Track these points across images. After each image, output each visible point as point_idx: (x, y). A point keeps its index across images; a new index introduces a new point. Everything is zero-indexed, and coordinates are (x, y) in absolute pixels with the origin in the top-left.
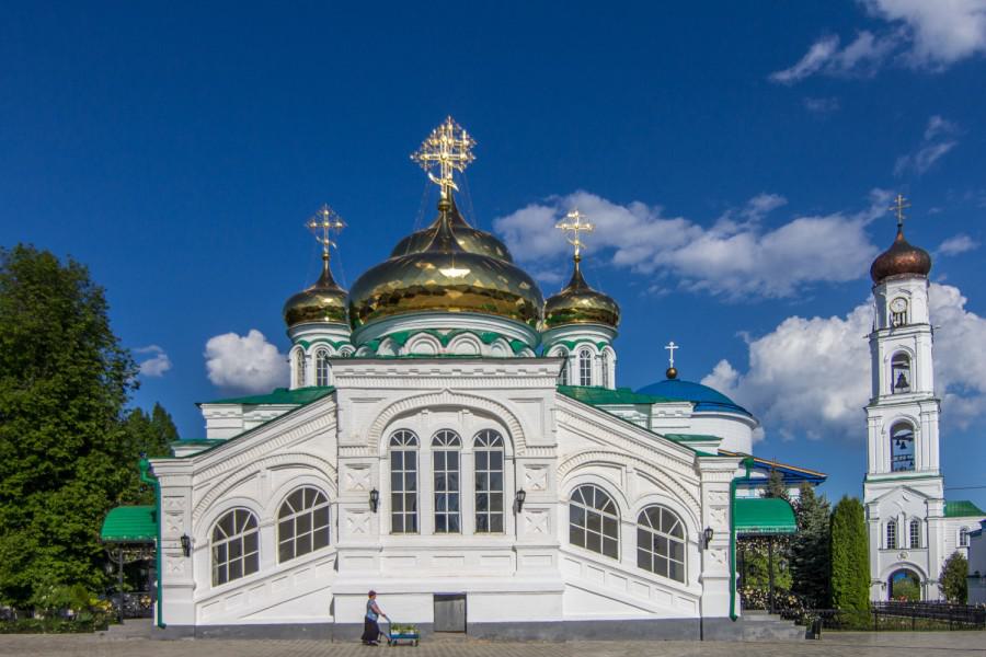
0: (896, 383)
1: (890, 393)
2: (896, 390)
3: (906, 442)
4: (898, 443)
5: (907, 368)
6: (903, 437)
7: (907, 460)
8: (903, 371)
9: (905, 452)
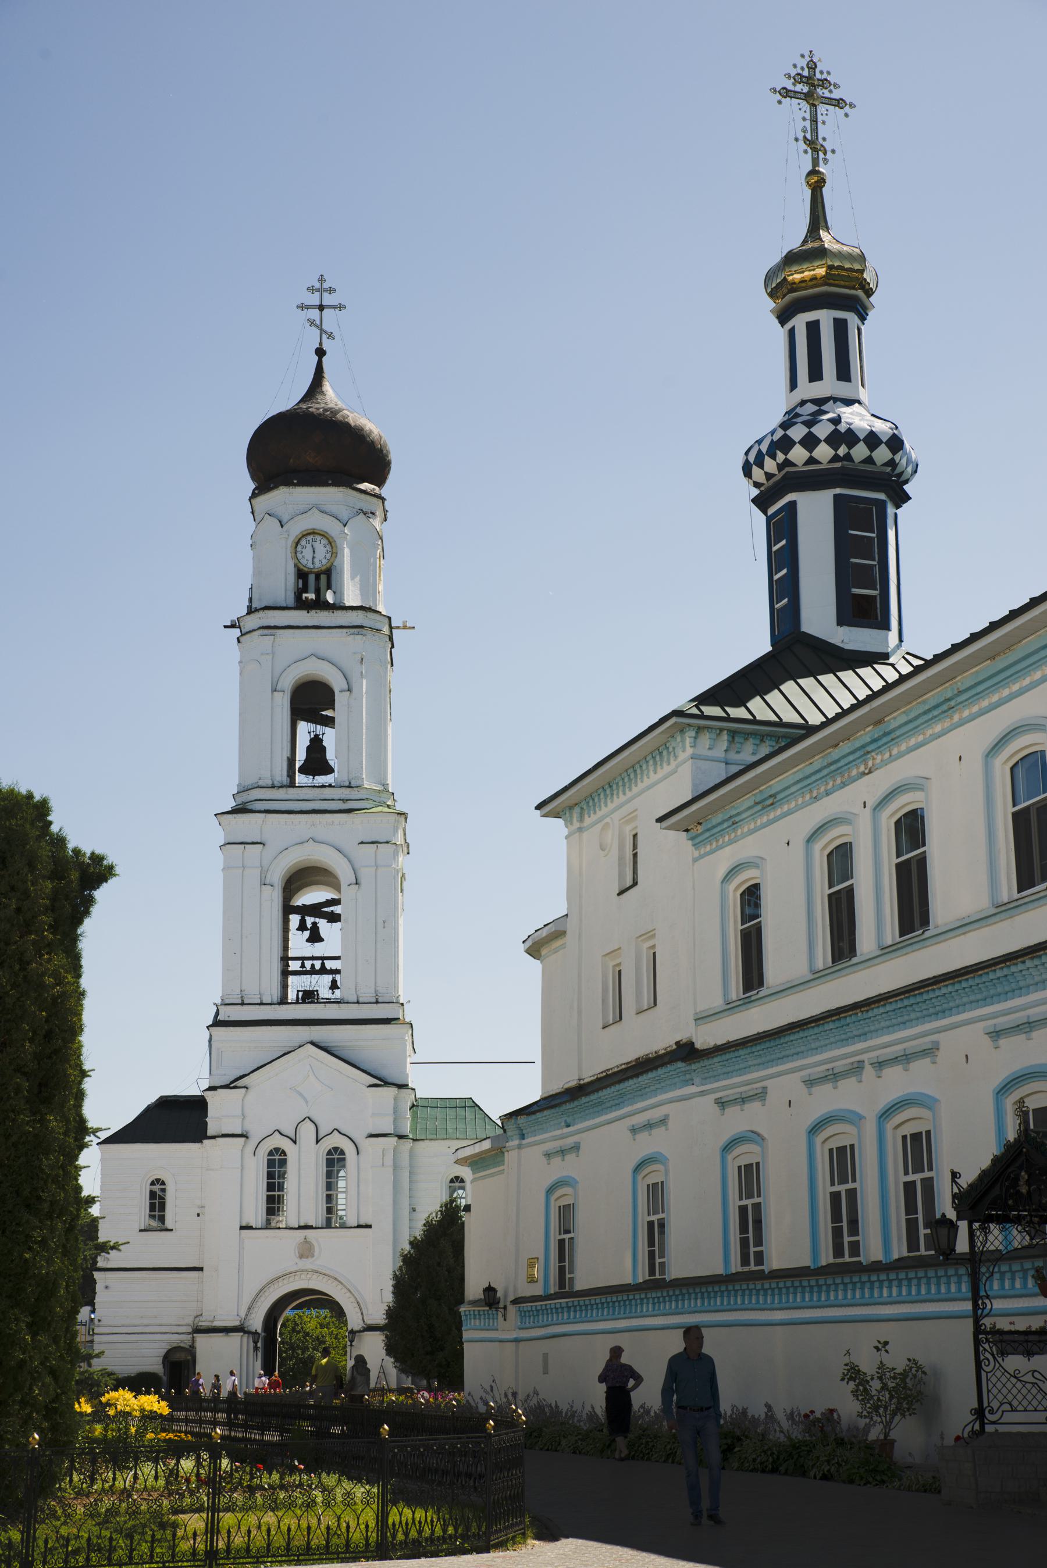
0: (301, 755)
1: (285, 780)
2: (300, 779)
3: (323, 924)
4: (302, 927)
5: (329, 722)
6: (315, 910)
7: (323, 971)
8: (319, 729)
9: (318, 950)
